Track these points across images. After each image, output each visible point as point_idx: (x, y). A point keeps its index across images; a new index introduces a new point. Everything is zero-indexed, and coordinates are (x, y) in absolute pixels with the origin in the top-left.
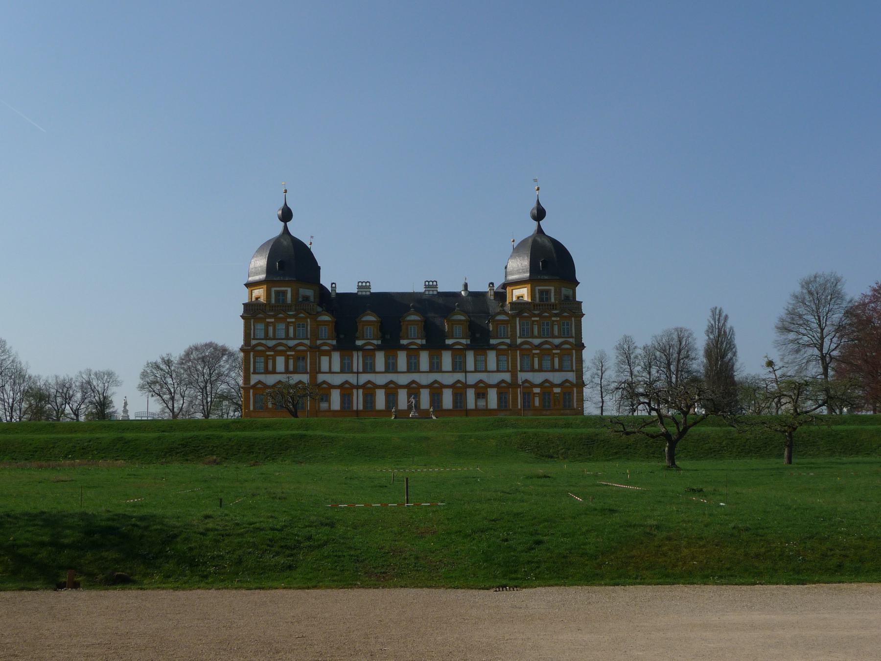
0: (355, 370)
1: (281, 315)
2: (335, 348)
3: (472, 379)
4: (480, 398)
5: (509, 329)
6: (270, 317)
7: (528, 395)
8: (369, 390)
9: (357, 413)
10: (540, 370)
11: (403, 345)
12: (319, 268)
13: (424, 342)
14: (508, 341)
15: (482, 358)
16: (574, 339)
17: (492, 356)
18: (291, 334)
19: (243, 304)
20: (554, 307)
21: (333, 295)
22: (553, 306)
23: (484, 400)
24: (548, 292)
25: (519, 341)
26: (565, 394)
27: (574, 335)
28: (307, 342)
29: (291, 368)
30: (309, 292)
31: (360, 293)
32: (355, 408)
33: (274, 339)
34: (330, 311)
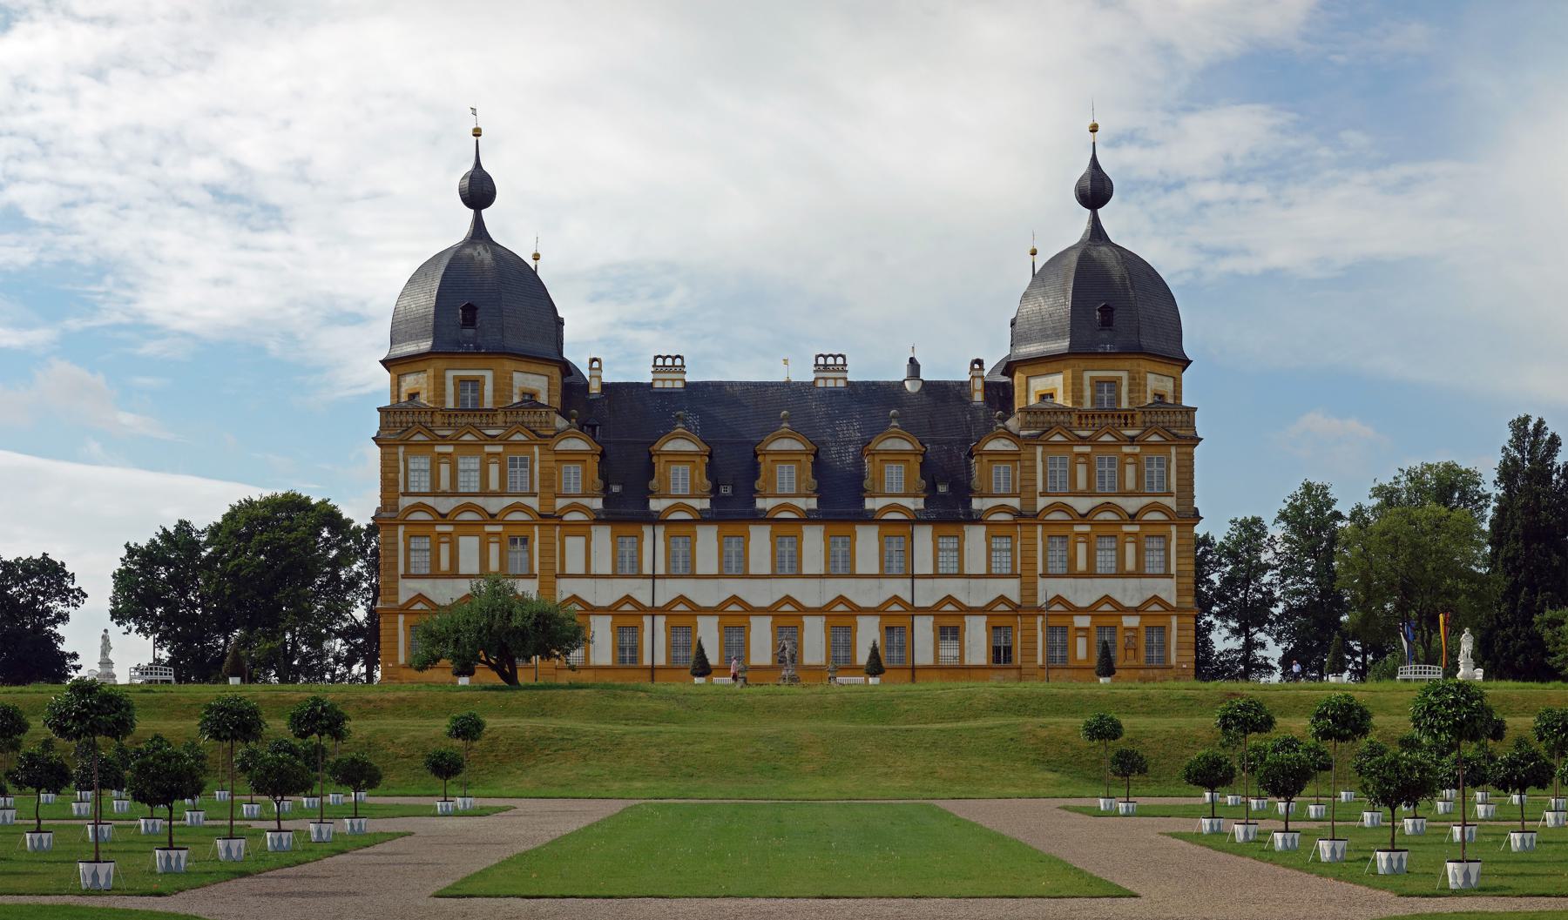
0: (647, 570)
1: (468, 438)
2: (599, 519)
3: (928, 593)
4: (946, 639)
5: (1018, 472)
6: (444, 440)
7: (1060, 632)
8: (682, 615)
9: (653, 668)
10: (1090, 574)
11: (763, 511)
12: (560, 323)
13: (812, 503)
14: (1015, 503)
15: (951, 543)
16: (1174, 499)
17: (975, 537)
18: (494, 485)
19: (379, 409)
20: (1129, 421)
22: (1126, 418)
23: (956, 643)
24: (1114, 384)
25: (1042, 503)
26: (1149, 629)
27: (1174, 488)
28: (533, 503)
30: (536, 382)
31: (658, 385)
32: (647, 662)
33: (455, 494)
34: (586, 427)
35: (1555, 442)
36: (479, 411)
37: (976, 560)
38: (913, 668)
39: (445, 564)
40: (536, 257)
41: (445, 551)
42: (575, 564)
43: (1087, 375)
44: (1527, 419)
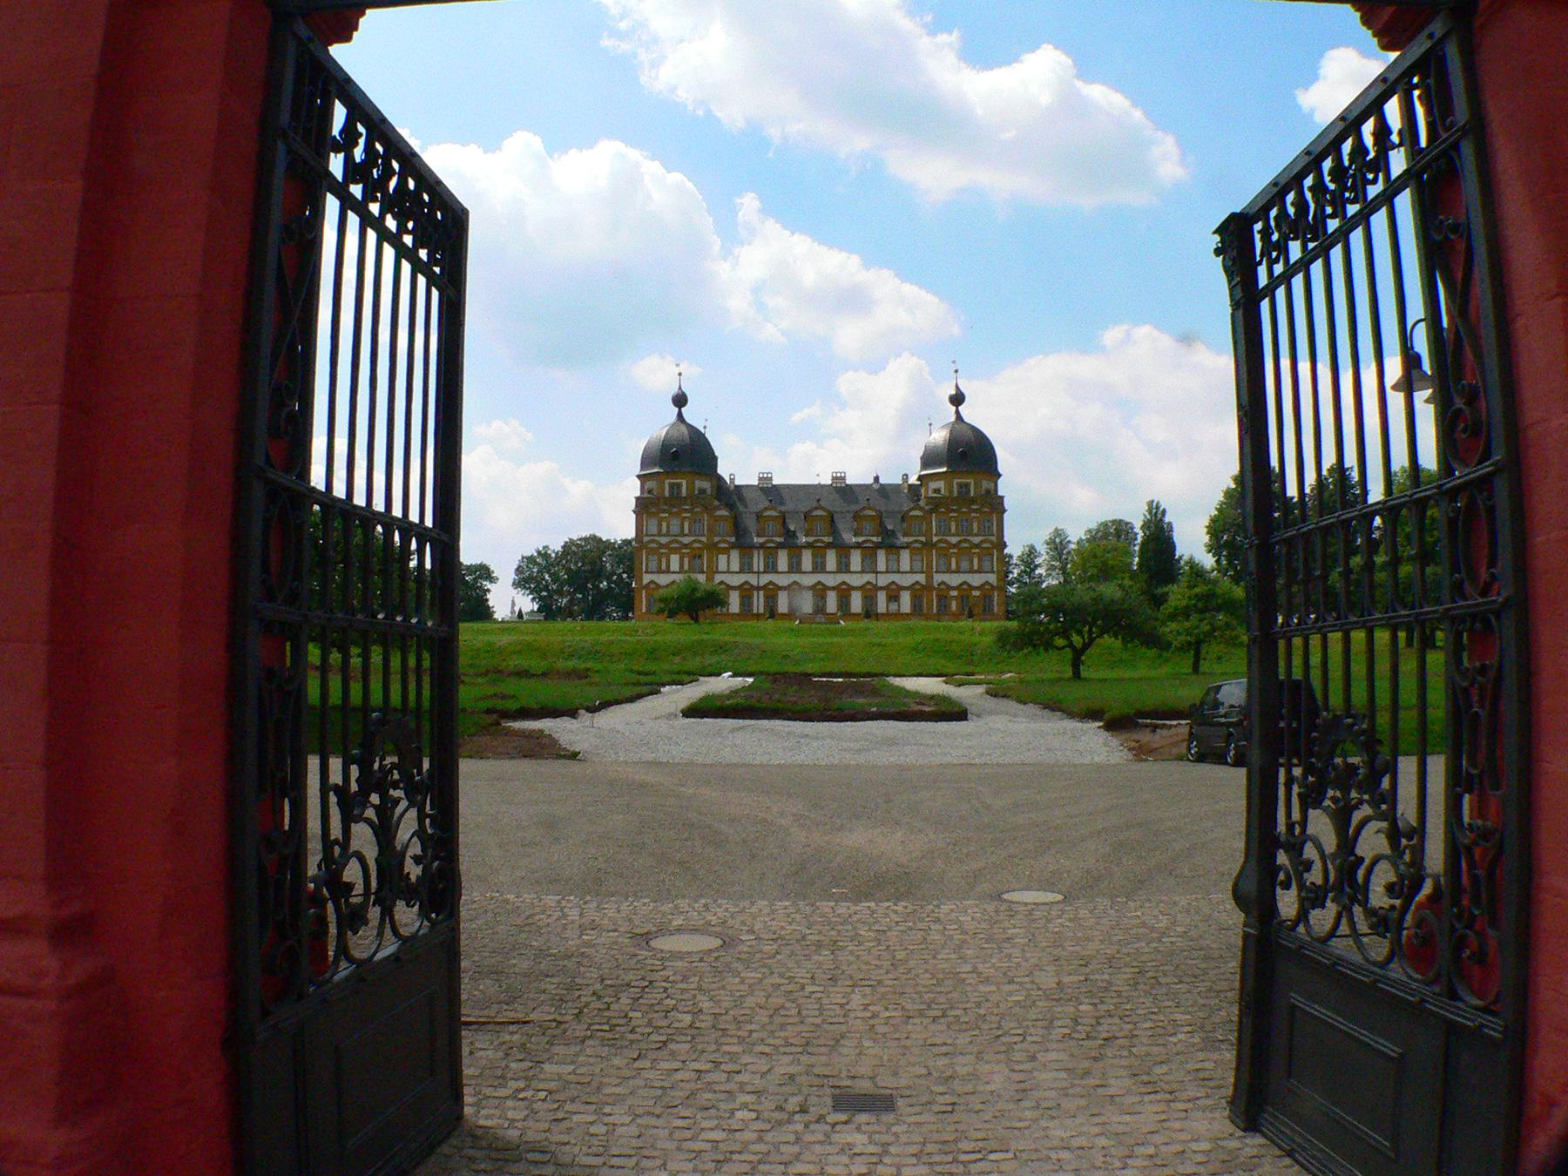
2: (733, 546)
3: (883, 581)
6: (664, 511)
7: (943, 599)
9: (758, 616)
10: (958, 571)
12: (715, 458)
14: (923, 539)
17: (905, 556)
18: (686, 531)
21: (732, 486)
25: (935, 539)
26: (985, 597)
28: (704, 539)
29: (686, 567)
30: (706, 485)
33: (667, 534)
35: (1164, 511)
36: (679, 497)
37: (905, 564)
38: (877, 614)
39: (664, 567)
40: (705, 427)
41: (664, 560)
42: (722, 565)
43: (955, 481)
44: (1153, 501)
